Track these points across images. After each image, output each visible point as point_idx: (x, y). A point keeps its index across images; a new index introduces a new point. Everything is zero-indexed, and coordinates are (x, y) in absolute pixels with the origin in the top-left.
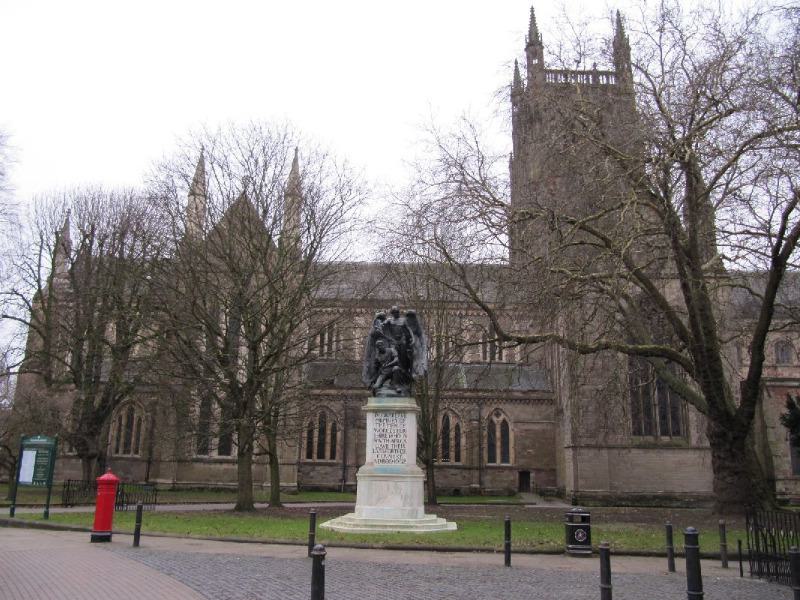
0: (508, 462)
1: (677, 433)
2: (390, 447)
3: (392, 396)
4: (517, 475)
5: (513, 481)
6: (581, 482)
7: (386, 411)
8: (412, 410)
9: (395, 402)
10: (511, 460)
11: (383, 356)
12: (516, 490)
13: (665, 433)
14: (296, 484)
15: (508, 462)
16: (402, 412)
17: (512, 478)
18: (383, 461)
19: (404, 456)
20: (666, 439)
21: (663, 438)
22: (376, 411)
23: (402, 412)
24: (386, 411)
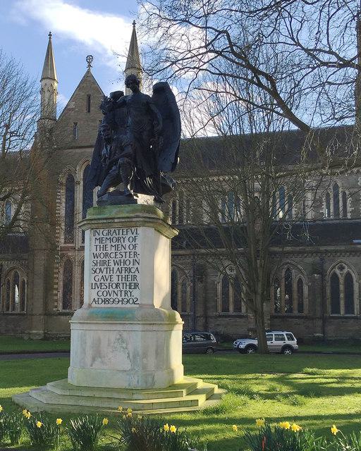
2: (115, 280)
18: (105, 301)
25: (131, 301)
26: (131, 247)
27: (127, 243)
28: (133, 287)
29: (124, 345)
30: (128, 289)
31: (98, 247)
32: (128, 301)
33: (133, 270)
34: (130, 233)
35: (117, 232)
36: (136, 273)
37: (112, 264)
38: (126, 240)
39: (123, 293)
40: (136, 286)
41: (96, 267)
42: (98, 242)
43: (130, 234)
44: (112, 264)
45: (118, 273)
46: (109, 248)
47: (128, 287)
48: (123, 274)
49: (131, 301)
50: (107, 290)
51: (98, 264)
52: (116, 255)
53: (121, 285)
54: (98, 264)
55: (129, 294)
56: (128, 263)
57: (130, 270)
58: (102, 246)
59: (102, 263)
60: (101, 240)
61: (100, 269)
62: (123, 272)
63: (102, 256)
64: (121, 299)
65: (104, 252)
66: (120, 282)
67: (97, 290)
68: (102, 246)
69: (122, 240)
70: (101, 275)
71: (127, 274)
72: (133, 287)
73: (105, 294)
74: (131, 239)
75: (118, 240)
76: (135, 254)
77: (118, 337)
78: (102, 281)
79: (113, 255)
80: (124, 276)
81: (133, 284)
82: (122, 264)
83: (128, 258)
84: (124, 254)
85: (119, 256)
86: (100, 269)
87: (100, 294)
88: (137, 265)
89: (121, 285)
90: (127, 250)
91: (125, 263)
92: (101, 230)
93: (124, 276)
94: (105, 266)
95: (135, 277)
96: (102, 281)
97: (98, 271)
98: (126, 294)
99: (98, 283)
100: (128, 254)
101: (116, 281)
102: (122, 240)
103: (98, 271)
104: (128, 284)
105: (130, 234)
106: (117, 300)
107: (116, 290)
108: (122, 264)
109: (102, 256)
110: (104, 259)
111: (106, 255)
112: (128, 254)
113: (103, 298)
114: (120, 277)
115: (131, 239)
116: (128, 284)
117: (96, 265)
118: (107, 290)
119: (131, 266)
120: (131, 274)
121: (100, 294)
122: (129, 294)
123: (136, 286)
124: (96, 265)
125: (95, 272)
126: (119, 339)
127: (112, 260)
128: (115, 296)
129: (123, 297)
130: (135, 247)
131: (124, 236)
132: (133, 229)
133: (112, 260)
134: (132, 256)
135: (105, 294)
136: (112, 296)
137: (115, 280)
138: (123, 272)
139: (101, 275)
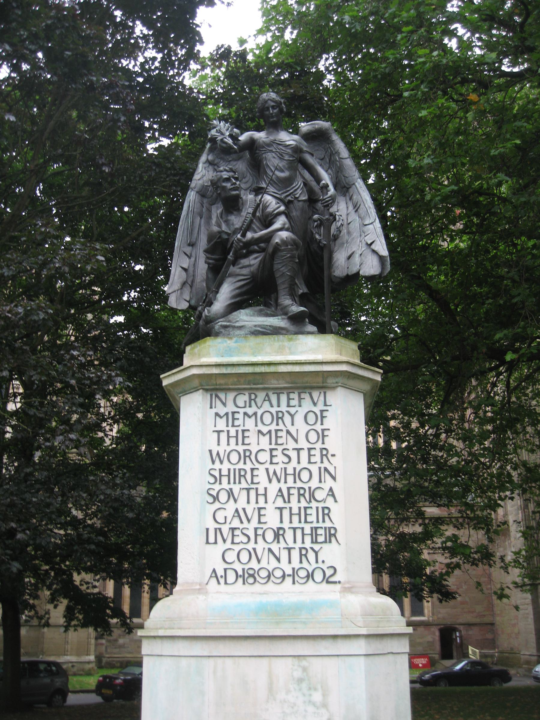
0: (422, 614)
2: (272, 519)
3: (276, 331)
4: (437, 633)
5: (431, 644)
7: (253, 382)
8: (346, 379)
9: (280, 350)
10: (426, 611)
11: (237, 221)
12: (437, 657)
14: (92, 658)
15: (422, 614)
16: (309, 382)
17: (429, 638)
18: (248, 577)
19: (331, 554)
22: (215, 384)
23: (309, 382)
24: (253, 382)
25: (318, 576)
26: (313, 437)
27: (300, 427)
28: (321, 539)
29: (317, 697)
30: (308, 543)
31: (224, 436)
33: (319, 495)
37: (262, 478)
38: (299, 419)
39: (295, 554)
40: (331, 535)
41: (217, 487)
42: (221, 424)
43: (307, 405)
45: (280, 503)
46: (252, 438)
47: (308, 539)
48: (294, 504)
49: (318, 576)
50: (250, 546)
51: (225, 480)
52: (272, 456)
53: (289, 535)
54: (225, 480)
55: (311, 556)
56: (305, 476)
57: (312, 495)
58: (233, 433)
59: (233, 477)
60: (231, 418)
61: (230, 493)
62: (294, 499)
63: (234, 457)
64: (289, 571)
65: (241, 448)
66: (286, 525)
67: (221, 547)
68: (233, 433)
69: (287, 419)
70: (231, 507)
71: (303, 504)
73: (244, 557)
74: (311, 418)
75: (278, 418)
76: (324, 454)
77: (298, 674)
78: (236, 523)
79: (264, 457)
80: (295, 511)
81: (320, 531)
82: (290, 479)
83: (304, 463)
84: (293, 455)
85: (280, 458)
86: (230, 493)
87: (231, 557)
88: (329, 482)
89: (289, 535)
90: (303, 444)
91: (297, 475)
92: (231, 396)
93: (295, 511)
94: (244, 485)
95: (326, 512)
96: (236, 523)
97: (223, 497)
98: (303, 555)
99: (225, 529)
100: (304, 455)
101: (276, 524)
102: (287, 419)
103: (223, 497)
104: (307, 531)
105: (307, 405)
106: (278, 573)
107: (275, 547)
108: (290, 479)
109: (234, 457)
110: (241, 465)
111: (246, 456)
112: (304, 455)
113: (239, 568)
114: (286, 513)
115: (311, 418)
116: (307, 531)
117: (218, 480)
119: (314, 483)
120: (314, 504)
121: (231, 557)
122: (311, 556)
123: (331, 535)
124: (218, 480)
125: (216, 498)
126: (300, 681)
127: (262, 468)
128: (274, 563)
129: (296, 564)
130: (322, 436)
131: (292, 410)
132: (315, 394)
133: (262, 468)
134: (317, 458)
135: (244, 557)
136: (264, 564)
137: (272, 519)
138: (294, 499)
139: (231, 507)
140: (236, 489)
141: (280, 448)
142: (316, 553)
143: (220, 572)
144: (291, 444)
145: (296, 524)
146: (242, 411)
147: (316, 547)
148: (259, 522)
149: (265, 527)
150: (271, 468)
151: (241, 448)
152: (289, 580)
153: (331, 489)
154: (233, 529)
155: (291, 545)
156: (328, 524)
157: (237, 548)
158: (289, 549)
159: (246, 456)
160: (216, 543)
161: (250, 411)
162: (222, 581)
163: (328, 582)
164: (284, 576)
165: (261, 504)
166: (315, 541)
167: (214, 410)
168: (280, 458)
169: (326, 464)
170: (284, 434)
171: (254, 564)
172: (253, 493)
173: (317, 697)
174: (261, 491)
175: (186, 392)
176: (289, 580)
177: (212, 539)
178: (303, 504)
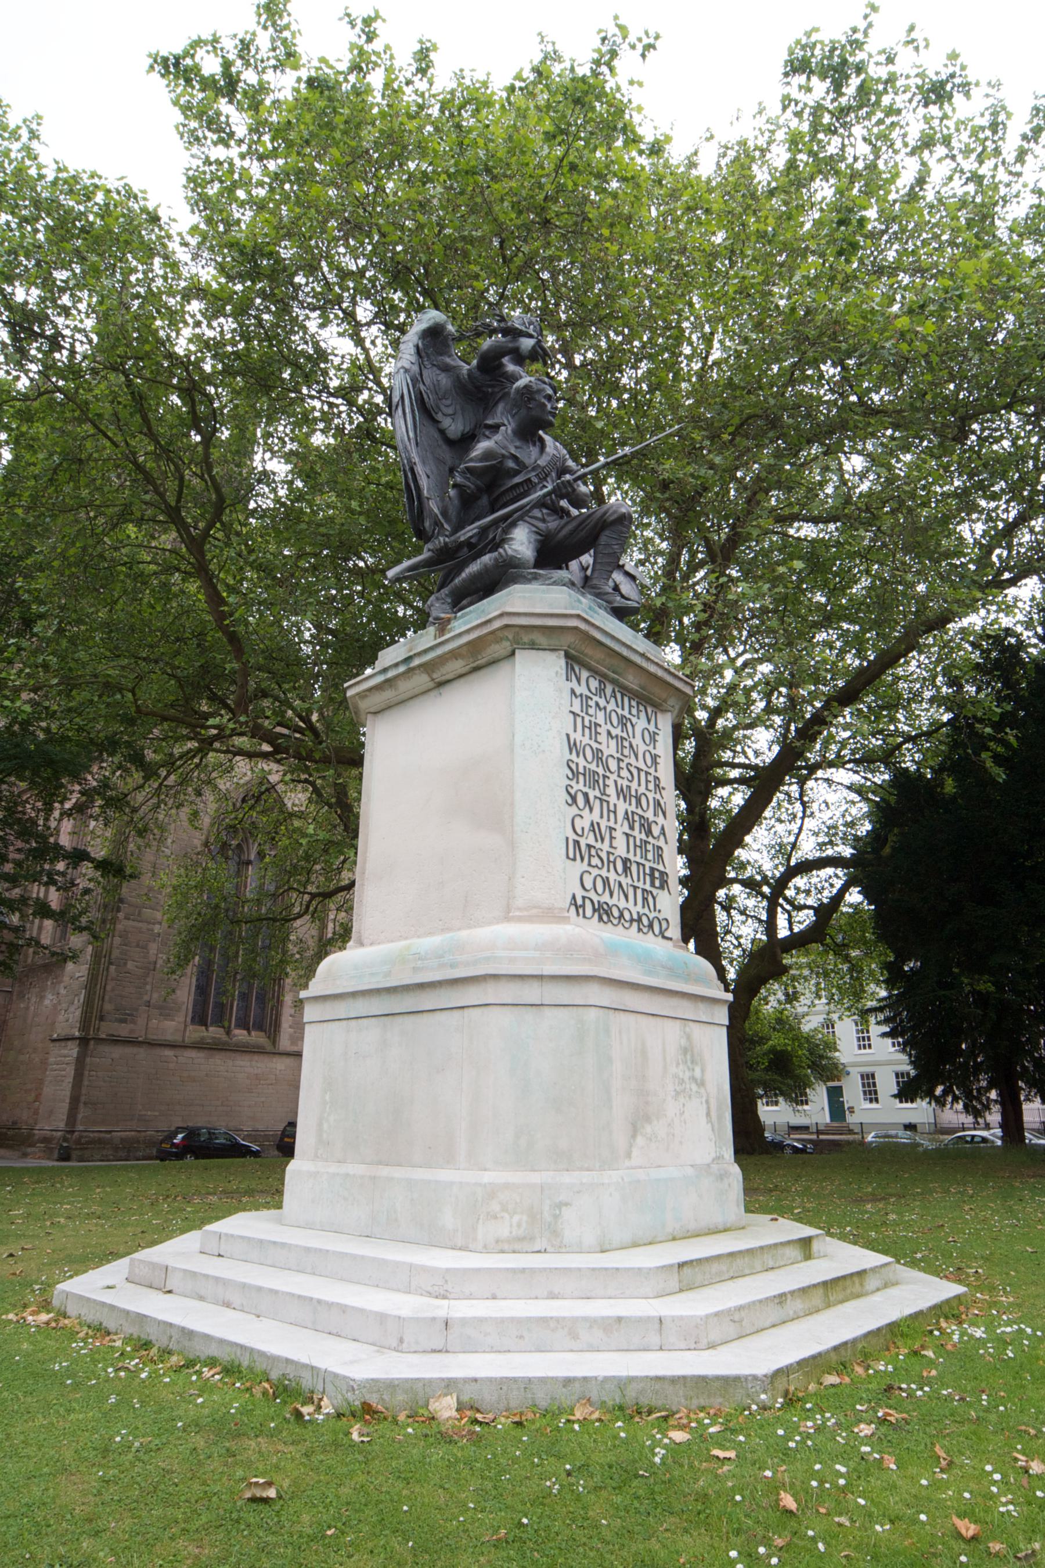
1: (260, 1027)
6: (82, 1112)
13: (243, 1024)
18: (603, 912)
20: (240, 1035)
21: (237, 1032)
28: (657, 883)
32: (651, 926)
34: (643, 715)
35: (619, 696)
36: (661, 843)
37: (611, 791)
44: (611, 791)
52: (619, 768)
62: (637, 825)
65: (595, 745)
66: (631, 856)
67: (580, 866)
72: (657, 883)
96: (591, 840)
99: (583, 842)
117: (575, 775)
118: (604, 873)
119: (650, 815)
125: (574, 799)
134: (651, 786)
138: (637, 825)
140: (592, 794)
141: (626, 760)
142: (654, 898)
143: (579, 902)
144: (633, 760)
145: (638, 859)
146: (596, 698)
147: (655, 891)
148: (611, 846)
149: (617, 853)
150: (620, 781)
151: (595, 745)
152: (635, 924)
153: (663, 828)
154: (589, 846)
155: (636, 884)
156: (661, 867)
157: (595, 872)
158: (635, 888)
159: (598, 755)
160: (574, 859)
161: (602, 702)
162: (581, 911)
163: (664, 937)
164: (632, 920)
165: (612, 824)
166: (653, 885)
167: (569, 685)
168: (624, 773)
169: (658, 796)
170: (626, 744)
171: (606, 897)
172: (605, 804)
173: (697, 1072)
174: (612, 808)
175: (533, 646)
176: (635, 924)
177: (571, 855)
178: (643, 836)
